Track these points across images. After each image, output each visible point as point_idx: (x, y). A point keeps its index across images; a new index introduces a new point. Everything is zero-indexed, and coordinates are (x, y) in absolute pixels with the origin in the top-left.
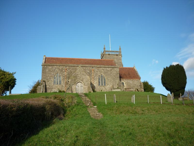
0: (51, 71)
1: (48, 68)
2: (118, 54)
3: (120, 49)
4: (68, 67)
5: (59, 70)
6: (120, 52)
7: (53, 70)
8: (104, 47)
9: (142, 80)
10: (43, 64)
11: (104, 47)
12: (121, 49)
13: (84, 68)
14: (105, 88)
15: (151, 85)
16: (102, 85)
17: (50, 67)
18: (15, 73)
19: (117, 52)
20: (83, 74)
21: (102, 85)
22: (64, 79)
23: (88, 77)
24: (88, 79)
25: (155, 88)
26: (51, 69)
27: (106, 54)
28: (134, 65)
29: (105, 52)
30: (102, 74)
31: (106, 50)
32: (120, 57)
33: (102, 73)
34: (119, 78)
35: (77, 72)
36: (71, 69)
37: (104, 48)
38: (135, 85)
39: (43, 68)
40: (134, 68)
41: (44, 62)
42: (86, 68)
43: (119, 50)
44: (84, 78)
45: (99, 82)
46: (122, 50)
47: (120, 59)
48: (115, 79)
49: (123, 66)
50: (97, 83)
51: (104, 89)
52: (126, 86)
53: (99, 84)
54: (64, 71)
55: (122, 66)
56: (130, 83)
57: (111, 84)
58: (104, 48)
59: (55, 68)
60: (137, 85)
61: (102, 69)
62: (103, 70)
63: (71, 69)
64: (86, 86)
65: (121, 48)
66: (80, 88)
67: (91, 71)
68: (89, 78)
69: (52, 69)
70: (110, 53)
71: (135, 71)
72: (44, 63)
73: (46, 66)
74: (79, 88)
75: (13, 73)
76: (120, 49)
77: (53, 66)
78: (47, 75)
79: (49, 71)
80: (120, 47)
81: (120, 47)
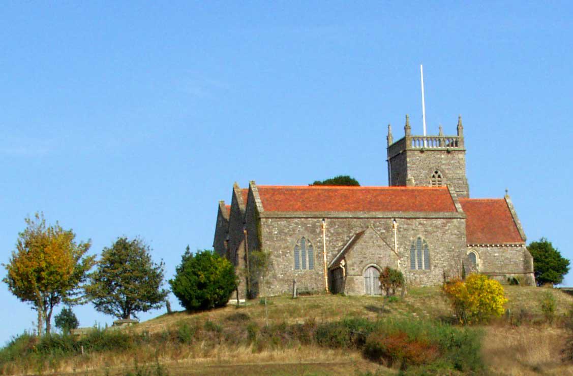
5: (307, 229)
9: (532, 236)
16: (420, 266)
17: (283, 223)
20: (381, 246)
21: (420, 266)
22: (319, 253)
26: (285, 226)
36: (337, 226)
37: (406, 128)
43: (453, 134)
44: (382, 256)
45: (413, 262)
46: (464, 133)
48: (453, 250)
53: (413, 266)
56: (495, 256)
59: (297, 223)
60: (515, 263)
61: (420, 224)
63: (337, 226)
68: (394, 255)
69: (288, 228)
73: (270, 220)
74: (370, 281)
77: (289, 220)
79: (281, 232)
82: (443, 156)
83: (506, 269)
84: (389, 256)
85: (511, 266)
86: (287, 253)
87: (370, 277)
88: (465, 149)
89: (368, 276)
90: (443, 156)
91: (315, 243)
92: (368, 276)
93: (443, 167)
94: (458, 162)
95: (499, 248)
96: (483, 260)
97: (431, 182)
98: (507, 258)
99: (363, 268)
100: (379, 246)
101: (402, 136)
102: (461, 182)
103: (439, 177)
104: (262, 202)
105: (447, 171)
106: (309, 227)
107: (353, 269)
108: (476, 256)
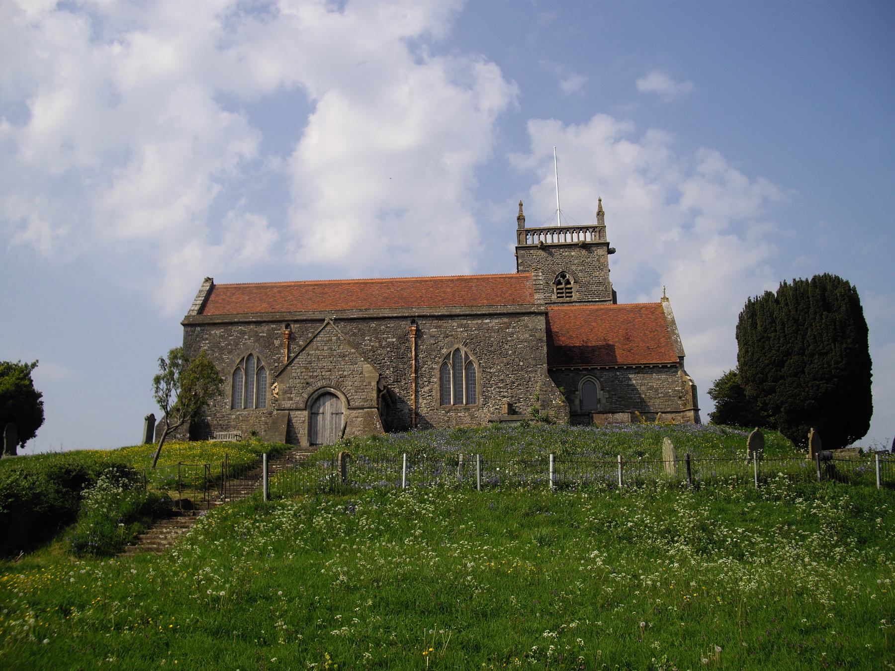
0: (222, 350)
1: (210, 335)
2: (589, 237)
3: (600, 214)
4: (297, 325)
5: (258, 339)
6: (599, 229)
7: (229, 344)
8: (521, 210)
10: (187, 317)
11: (521, 210)
12: (603, 214)
13: (373, 325)
14: (472, 417)
16: (458, 399)
18: (34, 365)
19: (585, 229)
20: (344, 356)
21: (458, 399)
23: (367, 367)
24: (368, 377)
26: (221, 337)
27: (529, 242)
29: (523, 236)
30: (456, 346)
31: (528, 226)
33: (460, 346)
34: (545, 365)
35: (317, 349)
37: (521, 219)
38: (657, 390)
39: (186, 332)
40: (664, 304)
41: (197, 308)
42: (380, 325)
43: (594, 222)
44: (345, 373)
47: (603, 267)
48: (522, 369)
49: (615, 301)
50: (434, 393)
51: (468, 420)
52: (604, 401)
53: (443, 400)
54: (277, 343)
55: (611, 298)
57: (504, 397)
58: (521, 219)
59: (243, 333)
60: (666, 394)
62: (465, 326)
64: (354, 413)
66: (331, 422)
67: (404, 339)
68: (369, 372)
69: (226, 339)
70: (549, 236)
71: (665, 319)
72: (195, 313)
73: (198, 329)
74: (324, 419)
75: (26, 366)
76: (600, 214)
80: (600, 207)
81: (600, 207)
82: (573, 254)
84: (361, 373)
85: (658, 401)
87: (323, 413)
88: (608, 241)
89: (334, 416)
90: (573, 254)
91: (269, 364)
92: (334, 416)
93: (574, 268)
94: (598, 260)
95: (637, 371)
96: (609, 392)
97: (555, 290)
98: (651, 388)
102: (601, 288)
103: (568, 282)
105: (580, 274)
106: (263, 337)
108: (597, 386)
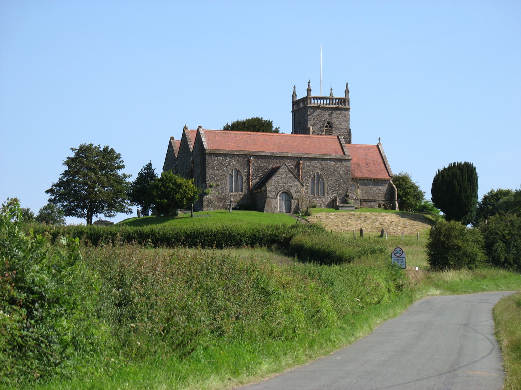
3: (347, 92)
8: (309, 86)
11: (309, 86)
12: (349, 92)
15: (417, 185)
16: (318, 193)
21: (318, 193)
25: (424, 193)
28: (379, 139)
31: (313, 94)
32: (346, 112)
37: (309, 90)
43: (343, 96)
45: (312, 190)
46: (351, 96)
58: (309, 90)
65: (349, 90)
76: (347, 92)
78: (217, 173)
79: (220, 164)
80: (347, 87)
81: (347, 87)
83: (377, 197)
86: (224, 179)
94: (345, 116)
96: (361, 189)
97: (324, 131)
99: (278, 193)
100: (290, 178)
101: (305, 95)
104: (207, 142)
107: (271, 194)
